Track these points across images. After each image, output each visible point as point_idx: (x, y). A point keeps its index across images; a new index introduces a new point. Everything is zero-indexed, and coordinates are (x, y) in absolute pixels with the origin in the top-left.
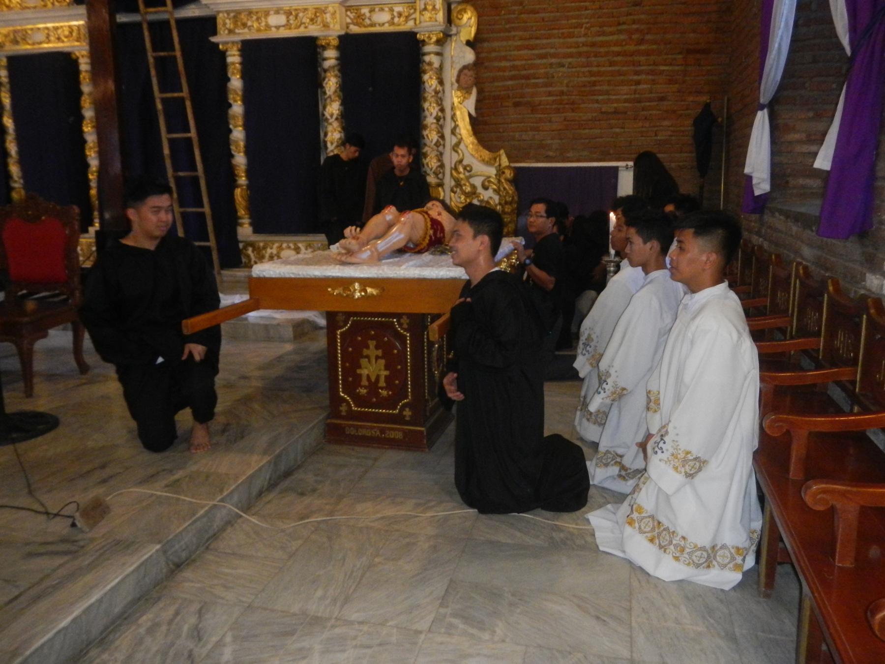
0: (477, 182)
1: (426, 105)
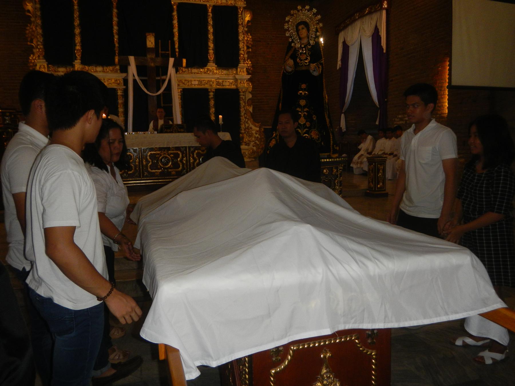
0: (254, 132)
1: (241, 110)
